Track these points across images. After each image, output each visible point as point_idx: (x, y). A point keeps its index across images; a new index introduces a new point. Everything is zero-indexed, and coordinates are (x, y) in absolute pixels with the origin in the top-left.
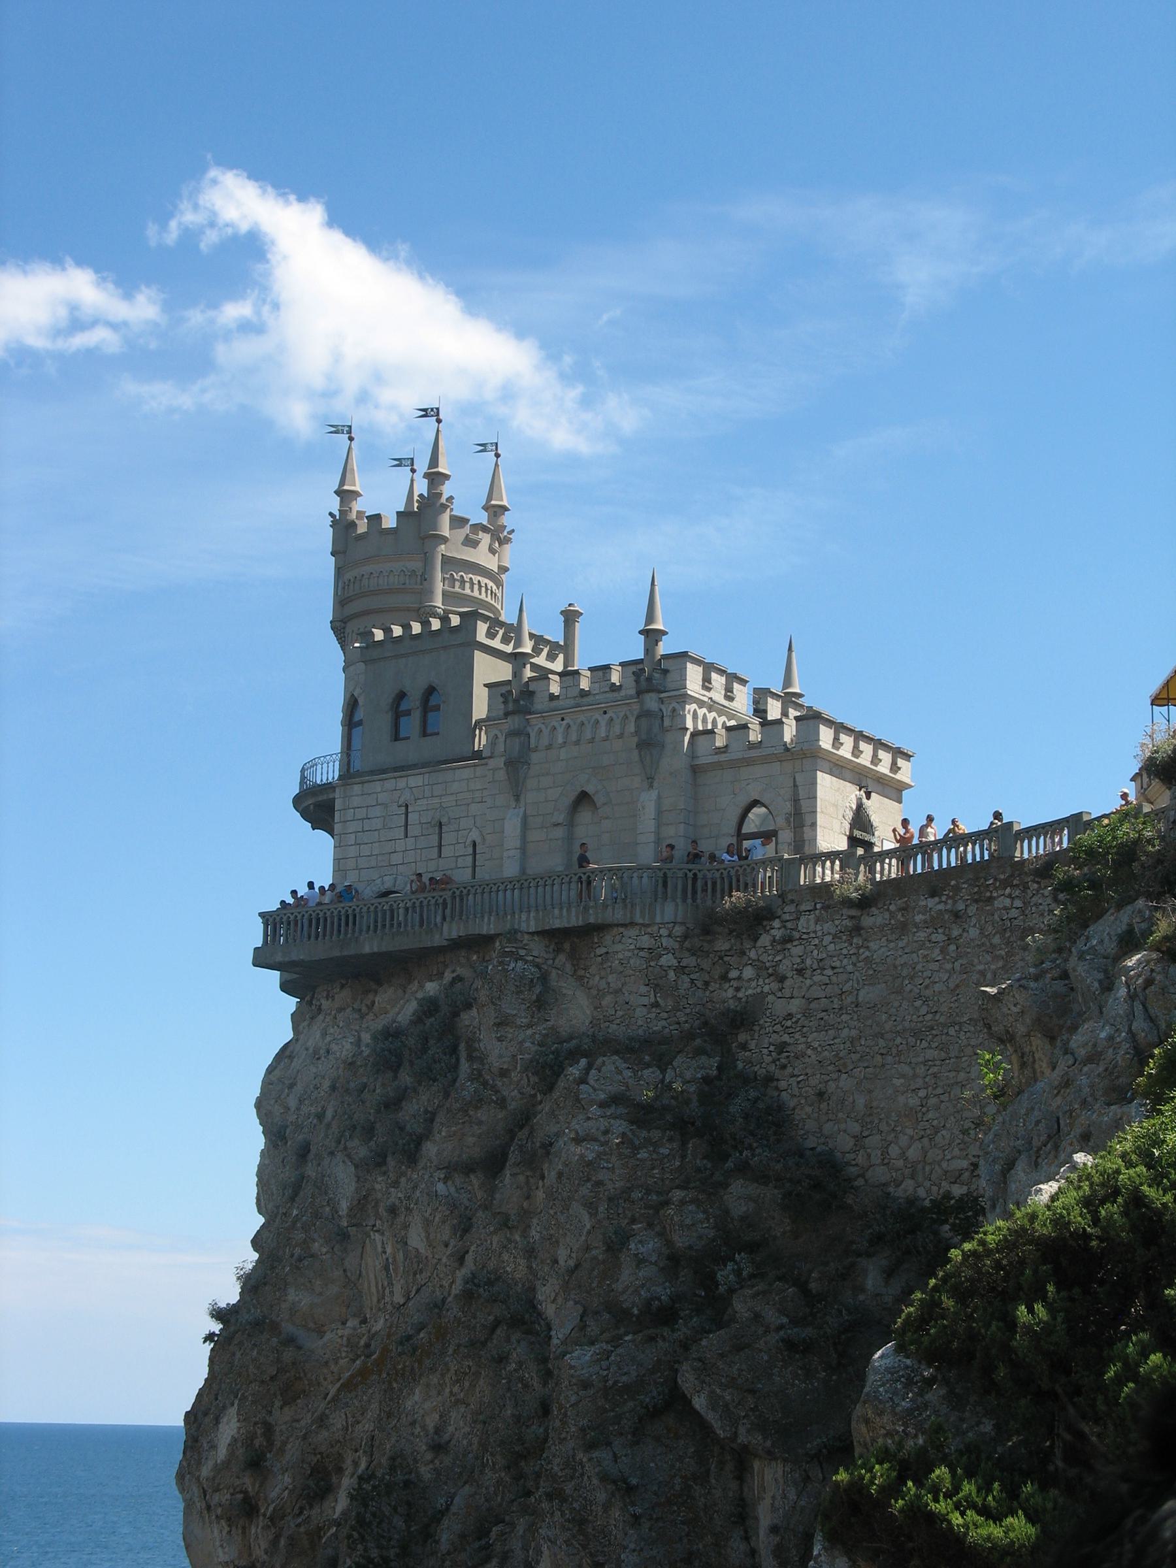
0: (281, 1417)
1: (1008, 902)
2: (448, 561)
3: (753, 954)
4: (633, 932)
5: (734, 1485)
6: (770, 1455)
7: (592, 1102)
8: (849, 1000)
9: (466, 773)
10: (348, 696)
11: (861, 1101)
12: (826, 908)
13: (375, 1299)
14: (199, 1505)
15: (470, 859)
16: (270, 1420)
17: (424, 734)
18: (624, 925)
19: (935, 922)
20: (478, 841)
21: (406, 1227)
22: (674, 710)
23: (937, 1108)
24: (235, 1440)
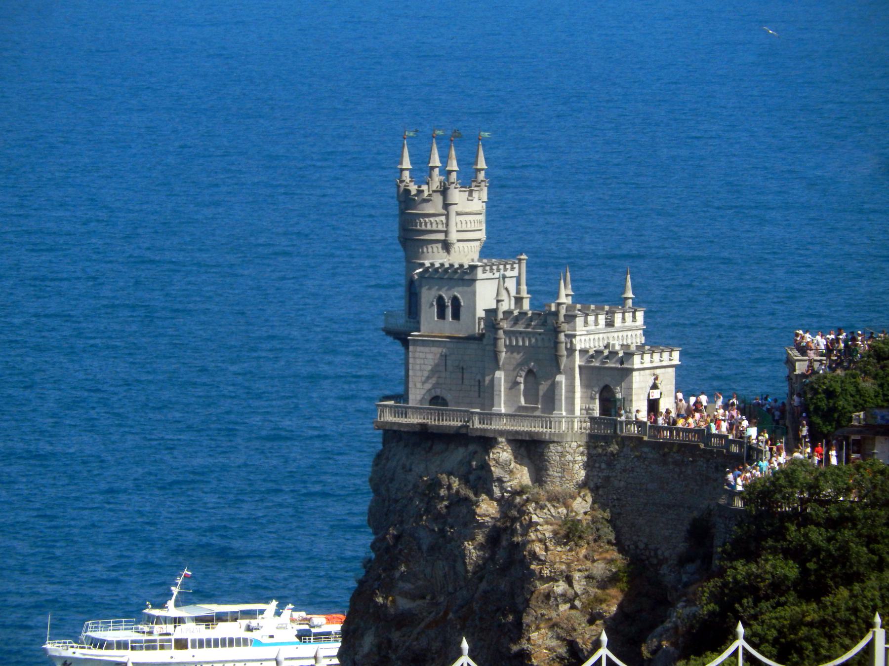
0: (396, 636)
2: (458, 214)
7: (537, 524)
15: (477, 388)
20: (481, 380)
21: (455, 561)
22: (571, 342)
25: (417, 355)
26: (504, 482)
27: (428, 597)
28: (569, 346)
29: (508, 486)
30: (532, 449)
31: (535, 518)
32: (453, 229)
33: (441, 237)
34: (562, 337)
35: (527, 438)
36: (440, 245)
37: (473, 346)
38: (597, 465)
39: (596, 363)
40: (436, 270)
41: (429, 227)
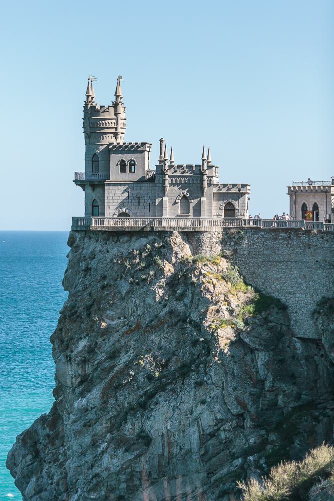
0: (100, 340)
1: (304, 238)
3: (234, 239)
4: (207, 233)
5: (251, 355)
6: (262, 350)
8: (261, 253)
9: (146, 185)
10: (94, 154)
11: (264, 275)
12: (255, 232)
13: (130, 313)
14: (64, 360)
16: (97, 341)
17: (130, 171)
18: (204, 232)
19: (284, 239)
21: (145, 298)
22: (210, 180)
23: (285, 278)
24: (85, 346)
25: (110, 191)
26: (178, 254)
27: (122, 318)
28: (209, 182)
29: (179, 256)
30: (192, 236)
31: (203, 272)
32: (120, 126)
33: (114, 130)
34: (205, 177)
35: (192, 230)
36: (112, 135)
37: (146, 185)
38: (228, 243)
39: (224, 190)
40: (121, 147)
41: (108, 126)
